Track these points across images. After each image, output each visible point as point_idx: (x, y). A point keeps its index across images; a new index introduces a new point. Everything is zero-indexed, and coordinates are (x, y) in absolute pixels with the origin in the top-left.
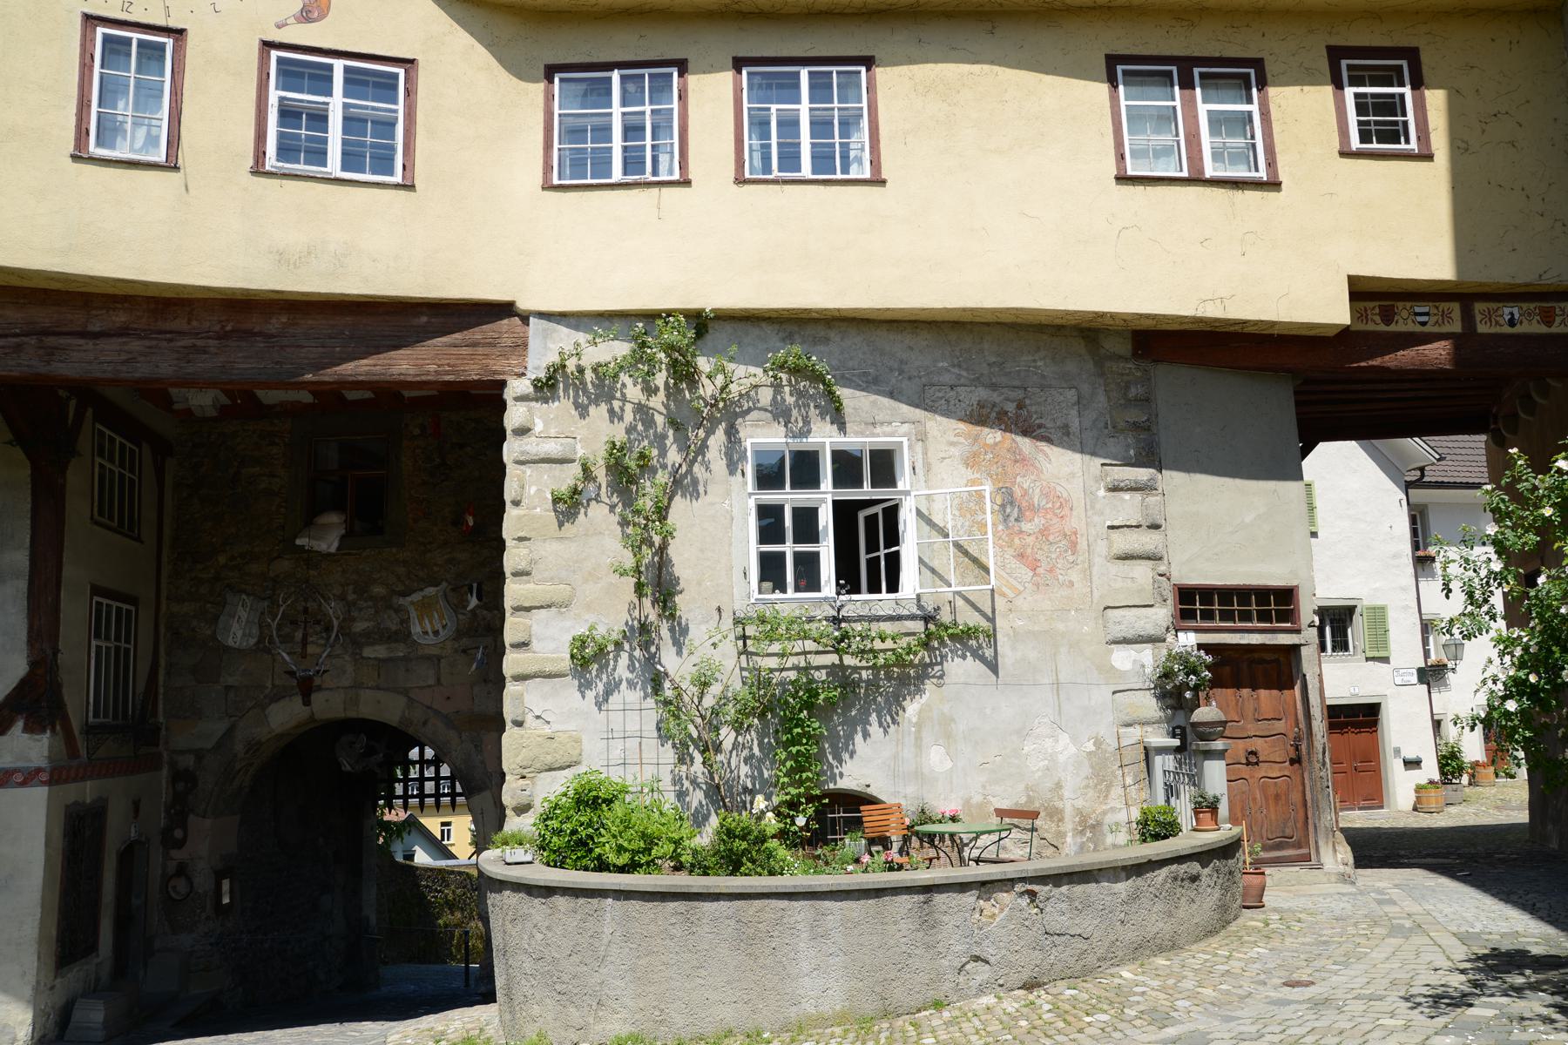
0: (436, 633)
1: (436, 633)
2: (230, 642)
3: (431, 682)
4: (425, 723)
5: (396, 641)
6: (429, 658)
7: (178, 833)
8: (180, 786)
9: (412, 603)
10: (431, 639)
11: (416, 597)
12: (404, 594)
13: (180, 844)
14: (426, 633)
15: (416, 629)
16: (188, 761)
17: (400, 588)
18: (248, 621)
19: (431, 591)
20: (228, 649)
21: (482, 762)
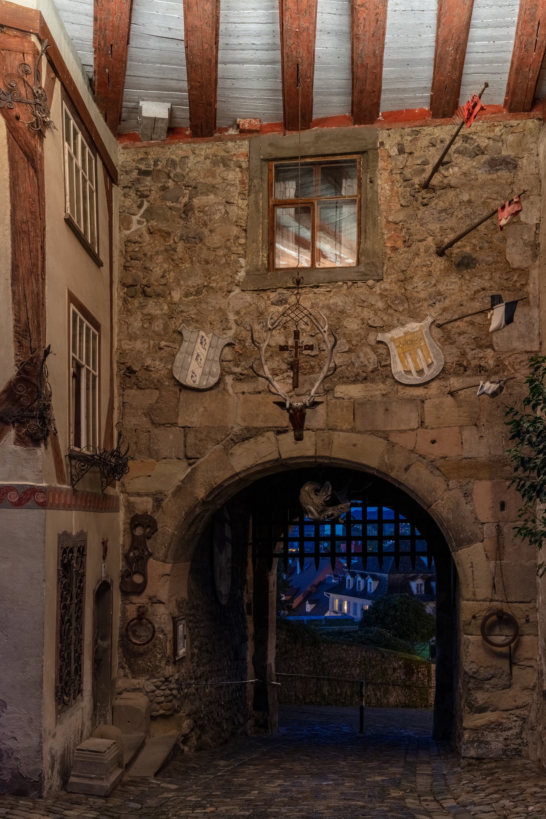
0: (420, 372)
1: (420, 372)
2: (189, 382)
3: (414, 424)
4: (407, 469)
5: (373, 381)
6: (411, 400)
7: (138, 579)
8: (139, 531)
9: (392, 340)
10: (415, 379)
11: (397, 333)
12: (383, 329)
13: (139, 589)
14: (409, 372)
15: (397, 368)
16: (145, 505)
17: (378, 323)
18: (207, 359)
19: (413, 326)
20: (183, 387)
21: (472, 512)
